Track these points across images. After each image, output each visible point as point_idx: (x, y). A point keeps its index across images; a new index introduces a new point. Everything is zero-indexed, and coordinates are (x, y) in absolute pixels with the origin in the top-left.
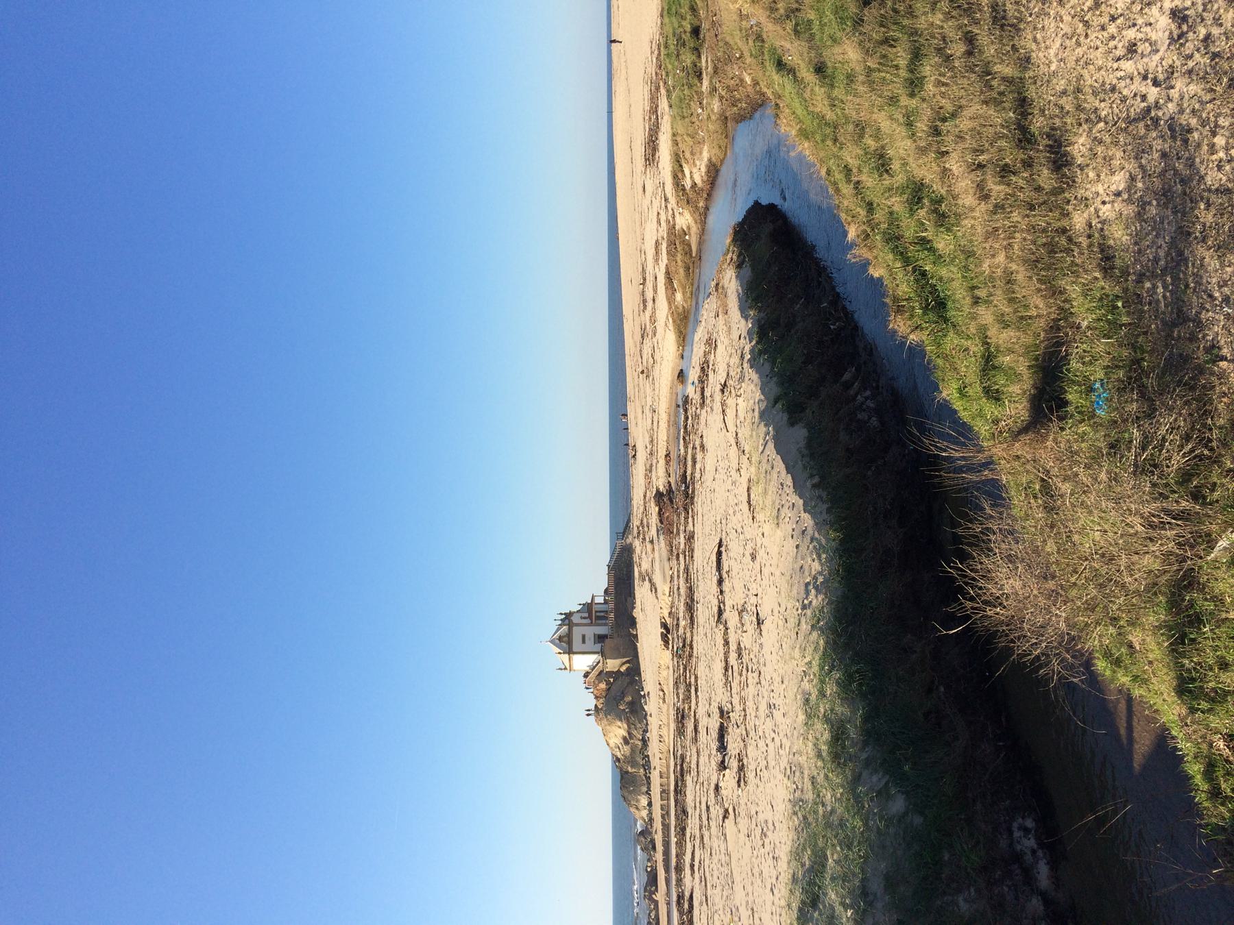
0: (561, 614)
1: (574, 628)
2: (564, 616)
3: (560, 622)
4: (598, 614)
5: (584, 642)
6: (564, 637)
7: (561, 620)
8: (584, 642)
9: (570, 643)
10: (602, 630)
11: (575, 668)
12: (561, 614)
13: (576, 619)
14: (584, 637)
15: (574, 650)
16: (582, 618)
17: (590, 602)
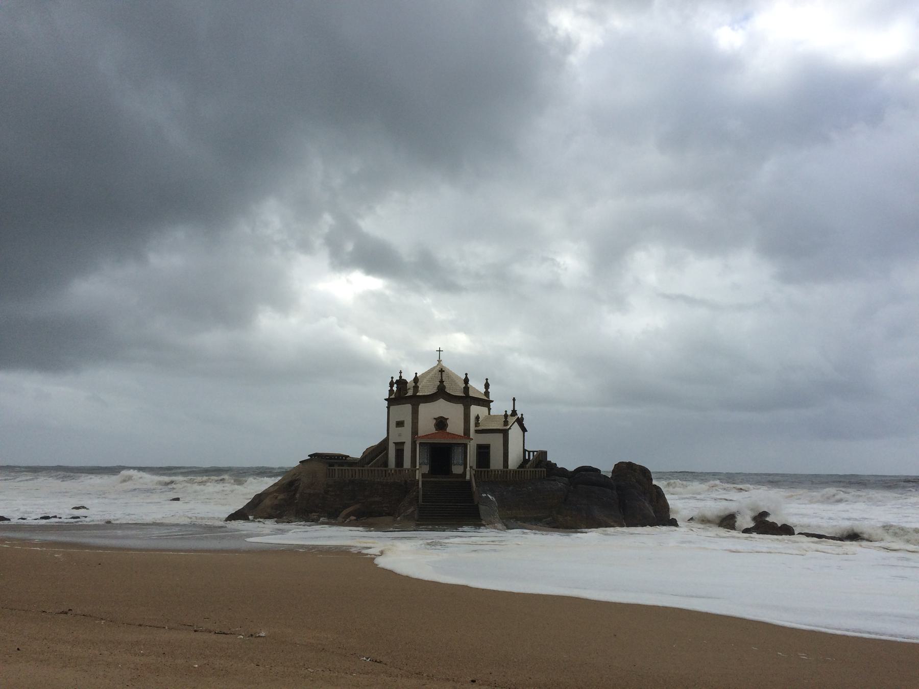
1: (407, 408)
6: (406, 390)
7: (442, 382)
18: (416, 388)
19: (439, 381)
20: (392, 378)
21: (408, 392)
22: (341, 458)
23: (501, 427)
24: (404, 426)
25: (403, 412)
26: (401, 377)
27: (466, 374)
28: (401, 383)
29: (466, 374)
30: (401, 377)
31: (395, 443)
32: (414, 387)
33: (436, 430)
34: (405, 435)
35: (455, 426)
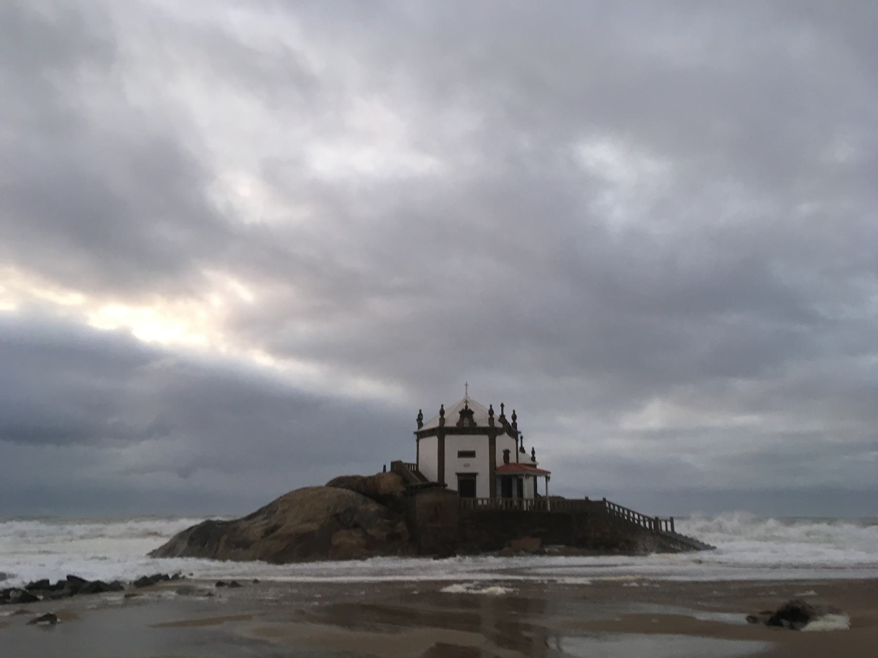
0: (514, 417)
1: (485, 439)
2: (510, 421)
3: (497, 413)
4: (515, 483)
5: (462, 454)
7: (502, 416)
8: (462, 454)
9: (459, 430)
10: (483, 490)
11: (422, 441)
12: (514, 417)
13: (504, 442)
14: (471, 454)
15: (449, 439)
16: (507, 453)
17: (538, 467)
18: (491, 420)
19: (500, 416)
20: (442, 406)
21: (476, 424)
22: (419, 487)
23: (530, 462)
24: (475, 456)
25: (479, 444)
26: (466, 407)
27: (514, 411)
28: (466, 413)
29: (514, 411)
30: (466, 407)
31: (459, 475)
32: (489, 419)
33: (505, 462)
34: (480, 466)
35: (512, 459)
